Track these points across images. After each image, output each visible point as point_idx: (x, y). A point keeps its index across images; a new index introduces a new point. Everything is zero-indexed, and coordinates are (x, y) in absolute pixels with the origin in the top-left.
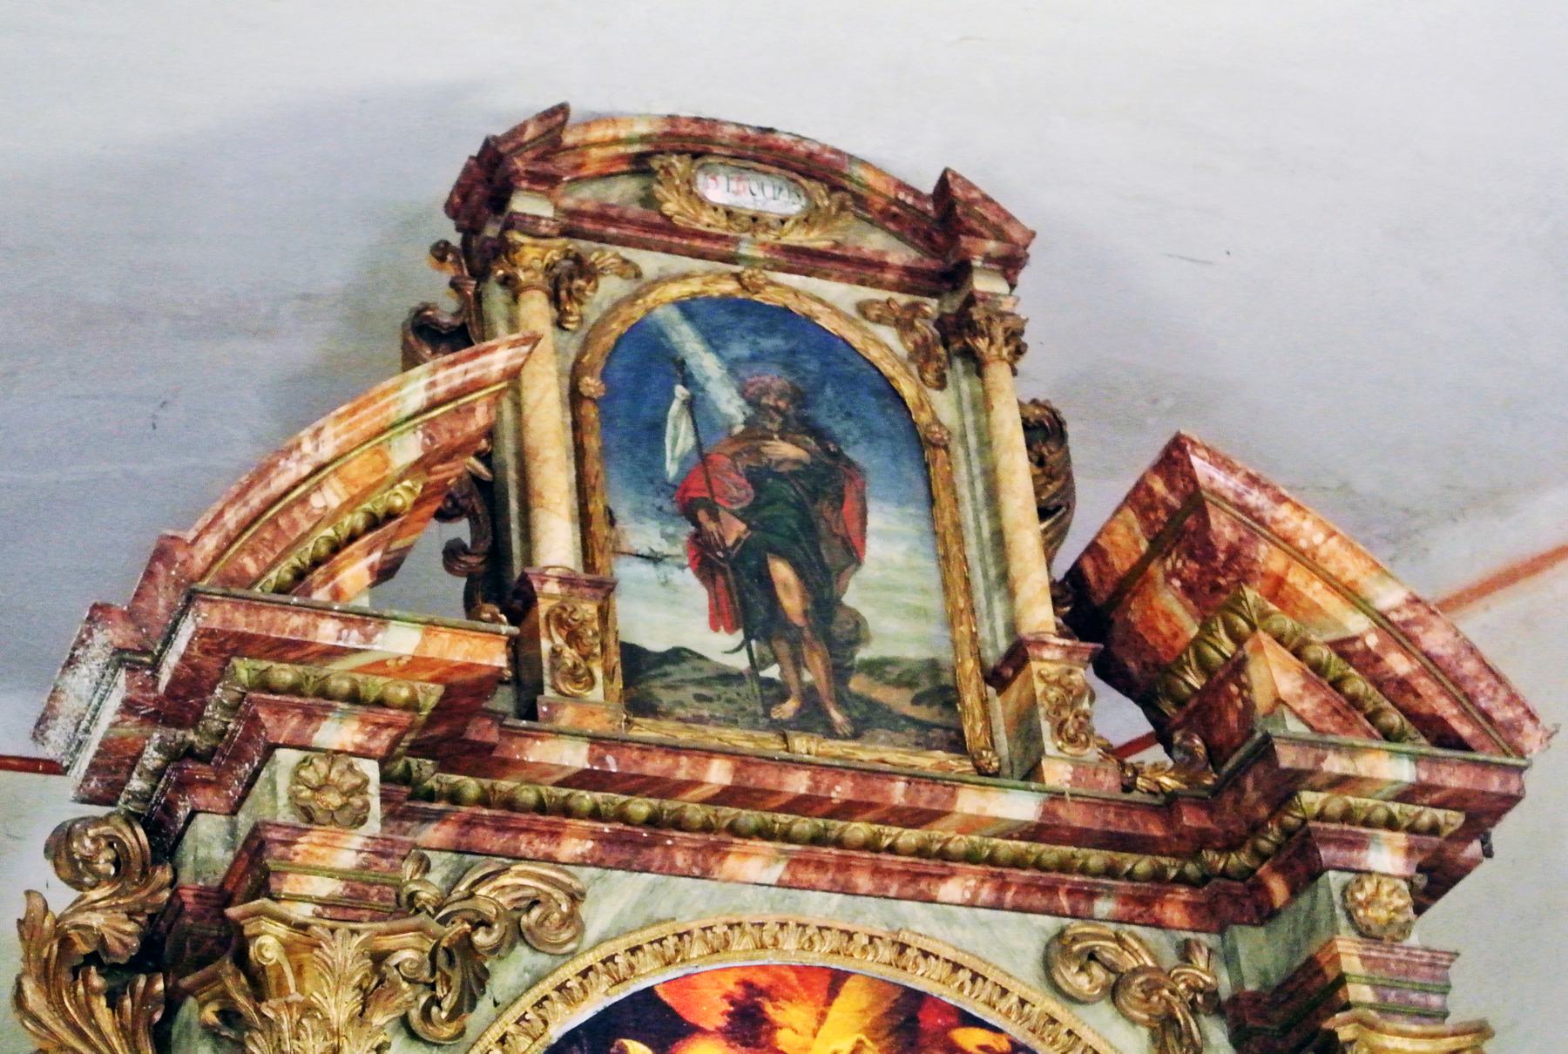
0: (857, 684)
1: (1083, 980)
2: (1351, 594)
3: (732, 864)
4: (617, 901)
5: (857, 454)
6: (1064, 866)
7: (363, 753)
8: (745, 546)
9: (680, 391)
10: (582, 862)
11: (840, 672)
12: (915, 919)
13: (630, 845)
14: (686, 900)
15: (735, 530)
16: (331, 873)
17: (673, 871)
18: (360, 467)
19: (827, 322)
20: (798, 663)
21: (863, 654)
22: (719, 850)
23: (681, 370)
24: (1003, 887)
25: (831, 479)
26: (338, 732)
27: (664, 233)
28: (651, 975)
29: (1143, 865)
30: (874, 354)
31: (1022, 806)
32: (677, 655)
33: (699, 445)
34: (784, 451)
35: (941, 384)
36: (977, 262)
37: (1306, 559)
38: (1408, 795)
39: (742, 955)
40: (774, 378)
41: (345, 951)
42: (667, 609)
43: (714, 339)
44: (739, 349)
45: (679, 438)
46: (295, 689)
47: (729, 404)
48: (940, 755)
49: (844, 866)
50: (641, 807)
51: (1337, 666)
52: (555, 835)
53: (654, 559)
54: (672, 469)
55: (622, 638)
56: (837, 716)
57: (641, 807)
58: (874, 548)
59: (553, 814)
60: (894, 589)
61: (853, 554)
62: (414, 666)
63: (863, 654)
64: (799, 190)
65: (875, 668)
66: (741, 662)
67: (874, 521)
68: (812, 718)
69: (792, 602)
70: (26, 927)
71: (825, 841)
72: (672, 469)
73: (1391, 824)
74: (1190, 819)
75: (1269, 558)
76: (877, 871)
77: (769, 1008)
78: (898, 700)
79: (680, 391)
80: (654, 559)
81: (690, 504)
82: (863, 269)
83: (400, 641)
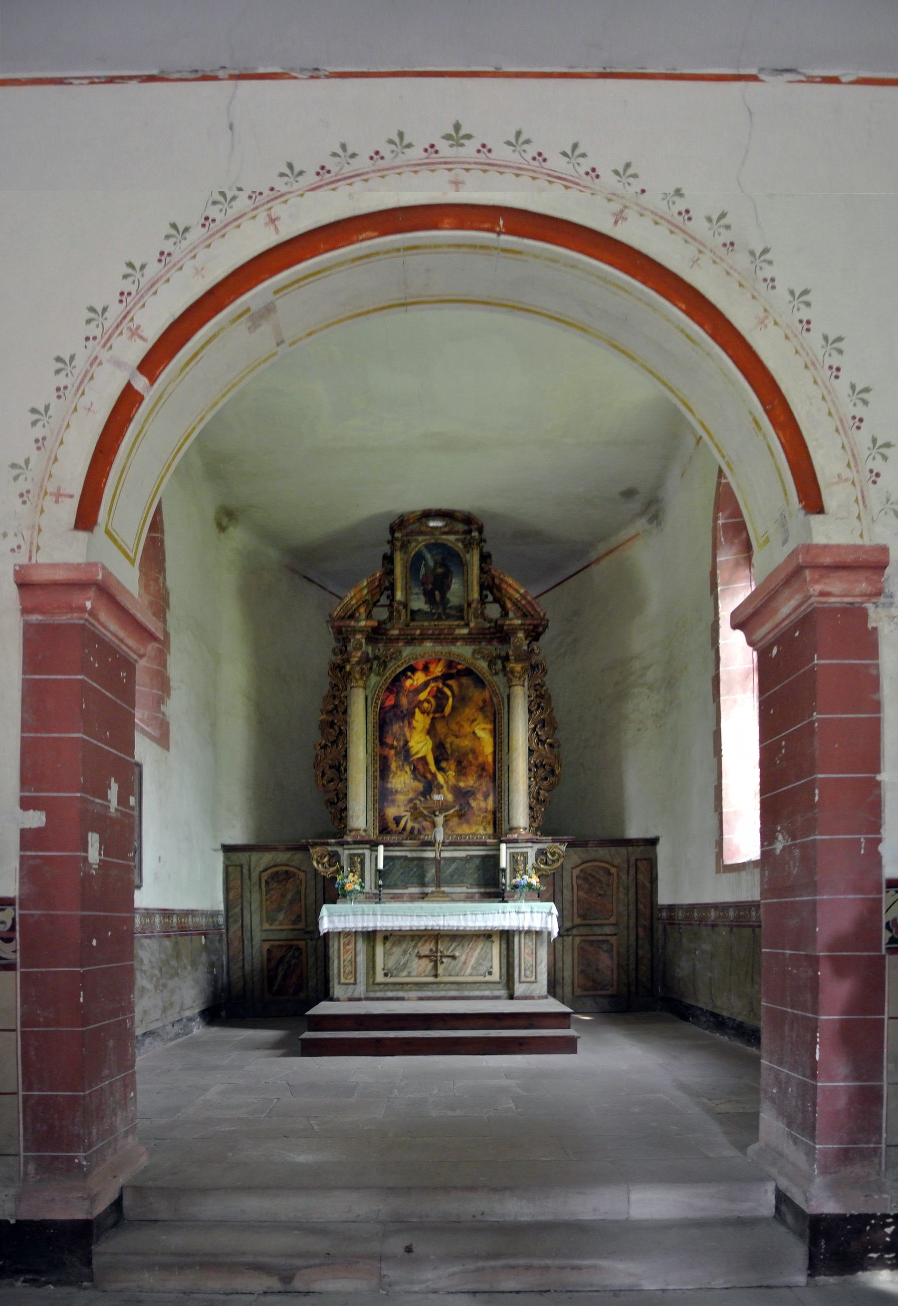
0: (447, 611)
4: (407, 651)
5: (452, 569)
11: (444, 609)
14: (418, 650)
15: (430, 586)
19: (450, 544)
23: (424, 558)
27: (421, 533)
28: (412, 662)
29: (489, 636)
31: (465, 631)
32: (419, 610)
34: (440, 570)
37: (510, 586)
38: (522, 624)
39: (427, 658)
40: (439, 557)
42: (419, 603)
43: (430, 552)
45: (423, 571)
47: (431, 563)
50: (409, 637)
53: (417, 594)
59: (397, 639)
61: (449, 588)
68: (440, 618)
69: (438, 598)
71: (438, 638)
73: (520, 629)
74: (492, 630)
75: (504, 586)
80: (417, 594)
81: (423, 584)
82: (456, 533)
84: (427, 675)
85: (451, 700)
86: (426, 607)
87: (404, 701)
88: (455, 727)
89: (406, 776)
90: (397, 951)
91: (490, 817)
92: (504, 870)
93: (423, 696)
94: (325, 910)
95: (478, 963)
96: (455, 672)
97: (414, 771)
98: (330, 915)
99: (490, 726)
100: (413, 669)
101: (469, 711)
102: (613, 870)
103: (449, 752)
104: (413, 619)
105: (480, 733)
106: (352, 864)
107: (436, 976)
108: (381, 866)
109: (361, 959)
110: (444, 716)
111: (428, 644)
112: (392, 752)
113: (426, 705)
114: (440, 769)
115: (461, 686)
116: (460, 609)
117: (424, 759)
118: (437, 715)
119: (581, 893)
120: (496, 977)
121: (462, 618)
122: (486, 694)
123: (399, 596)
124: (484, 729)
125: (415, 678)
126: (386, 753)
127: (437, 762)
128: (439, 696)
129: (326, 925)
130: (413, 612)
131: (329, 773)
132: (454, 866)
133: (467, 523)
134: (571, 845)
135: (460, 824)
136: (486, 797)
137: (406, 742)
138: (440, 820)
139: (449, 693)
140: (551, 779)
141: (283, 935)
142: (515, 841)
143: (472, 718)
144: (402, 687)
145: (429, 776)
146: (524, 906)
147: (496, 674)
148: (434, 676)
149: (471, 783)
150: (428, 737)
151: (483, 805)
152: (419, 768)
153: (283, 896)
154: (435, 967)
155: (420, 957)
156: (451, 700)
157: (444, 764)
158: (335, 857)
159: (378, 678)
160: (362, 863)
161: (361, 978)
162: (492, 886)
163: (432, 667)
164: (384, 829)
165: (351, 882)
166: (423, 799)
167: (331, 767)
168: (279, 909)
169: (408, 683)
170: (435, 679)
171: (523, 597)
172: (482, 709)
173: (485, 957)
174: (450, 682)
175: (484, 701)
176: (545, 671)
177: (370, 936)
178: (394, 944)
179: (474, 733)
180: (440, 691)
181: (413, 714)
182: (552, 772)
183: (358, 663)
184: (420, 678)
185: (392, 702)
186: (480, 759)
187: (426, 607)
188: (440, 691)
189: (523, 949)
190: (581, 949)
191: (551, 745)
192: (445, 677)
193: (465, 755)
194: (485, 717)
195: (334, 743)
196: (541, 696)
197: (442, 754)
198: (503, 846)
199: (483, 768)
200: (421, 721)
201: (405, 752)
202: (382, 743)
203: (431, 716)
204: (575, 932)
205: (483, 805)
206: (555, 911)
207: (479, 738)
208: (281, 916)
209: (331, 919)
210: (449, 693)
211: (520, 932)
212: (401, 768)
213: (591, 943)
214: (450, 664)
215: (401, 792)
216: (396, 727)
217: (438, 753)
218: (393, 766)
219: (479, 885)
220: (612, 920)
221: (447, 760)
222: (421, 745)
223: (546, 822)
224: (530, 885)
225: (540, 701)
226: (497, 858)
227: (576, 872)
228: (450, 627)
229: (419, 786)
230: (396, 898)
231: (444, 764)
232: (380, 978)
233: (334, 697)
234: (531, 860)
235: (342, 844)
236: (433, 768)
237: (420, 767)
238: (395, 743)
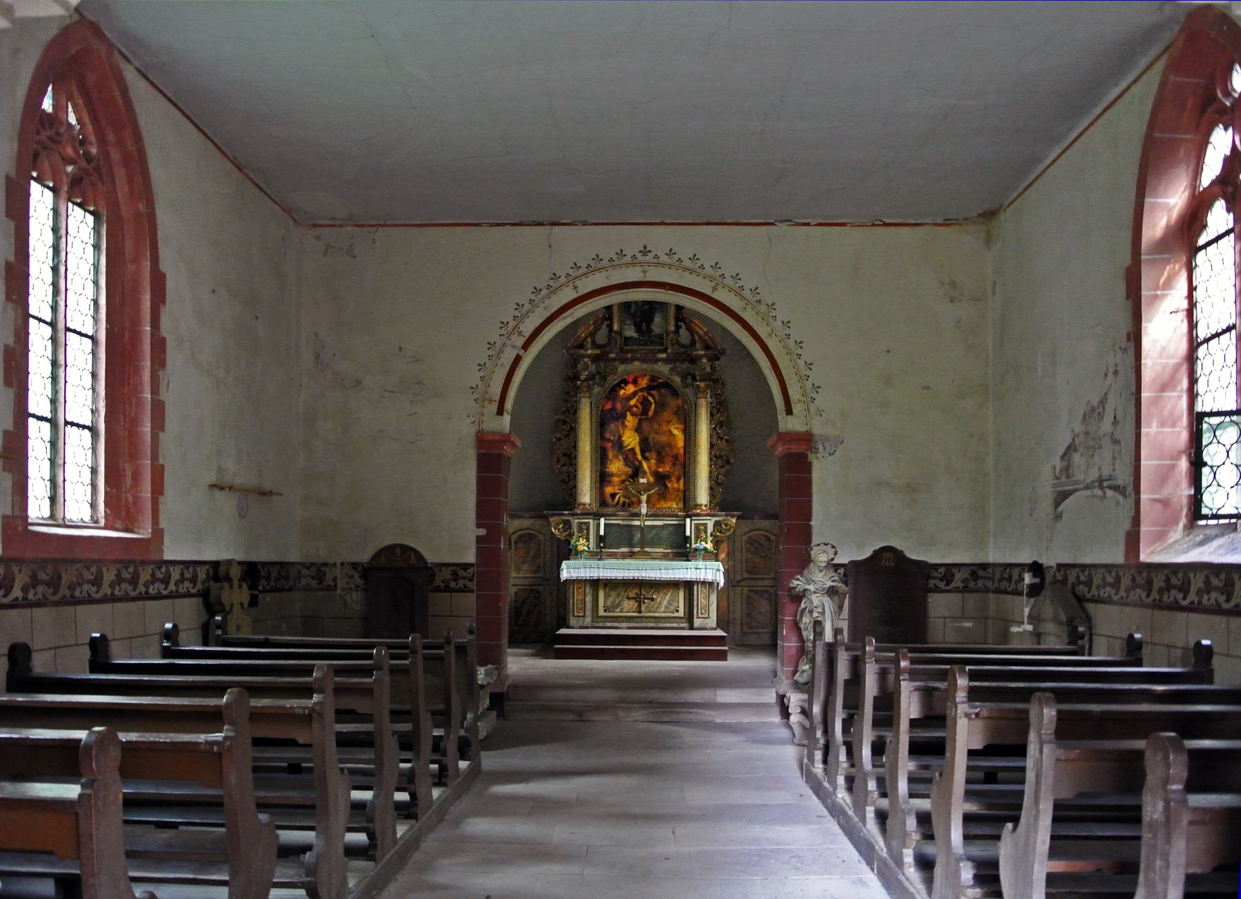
4: (621, 368)
14: (630, 367)
31: (664, 356)
42: (631, 332)
61: (653, 320)
68: (646, 344)
81: (633, 317)
86: (635, 335)
87: (619, 406)
90: (614, 594)
91: (681, 495)
92: (690, 538)
93: (633, 402)
94: (564, 564)
95: (669, 604)
96: (657, 384)
97: (625, 459)
98: (568, 568)
99: (681, 426)
100: (625, 382)
101: (667, 415)
102: (773, 538)
104: (626, 344)
105: (675, 432)
106: (580, 530)
107: (640, 612)
108: (602, 533)
109: (589, 599)
111: (637, 364)
114: (645, 458)
115: (661, 395)
116: (660, 337)
117: (633, 450)
119: (749, 555)
120: (681, 614)
121: (662, 344)
122: (680, 402)
123: (616, 327)
127: (643, 452)
128: (645, 403)
129: (564, 575)
130: (626, 339)
131: (563, 460)
132: (654, 532)
134: (739, 518)
135: (659, 500)
136: (678, 480)
137: (620, 437)
138: (644, 498)
140: (728, 467)
141: (526, 582)
142: (699, 515)
144: (618, 396)
146: (701, 564)
151: (676, 486)
152: (629, 457)
153: (528, 553)
154: (640, 606)
155: (629, 599)
157: (647, 454)
158: (568, 525)
160: (588, 529)
161: (588, 613)
162: (682, 550)
164: (603, 503)
165: (582, 545)
167: (564, 455)
168: (524, 563)
169: (622, 392)
170: (642, 390)
171: (706, 333)
172: (676, 413)
173: (674, 599)
175: (678, 408)
176: (724, 384)
177: (595, 583)
178: (611, 589)
180: (645, 399)
181: (625, 417)
182: (728, 462)
183: (586, 380)
184: (631, 389)
186: (675, 451)
187: (635, 335)
188: (645, 399)
189: (700, 594)
190: (749, 596)
191: (727, 441)
192: (649, 388)
193: (663, 447)
195: (566, 436)
196: (721, 403)
198: (688, 520)
199: (676, 457)
200: (631, 421)
201: (619, 445)
202: (602, 437)
204: (744, 583)
205: (676, 486)
206: (721, 568)
208: (525, 567)
209: (569, 570)
211: (697, 582)
212: (616, 457)
213: (756, 592)
214: (653, 378)
215: (616, 475)
216: (612, 426)
218: (610, 455)
219: (672, 547)
220: (772, 575)
222: (631, 439)
223: (723, 501)
224: (705, 549)
225: (719, 410)
226: (684, 525)
227: (745, 538)
228: (652, 351)
229: (629, 470)
230: (613, 556)
231: (647, 454)
232: (601, 613)
233: (566, 401)
234: (710, 529)
235: (573, 515)
236: (640, 457)
237: (630, 457)
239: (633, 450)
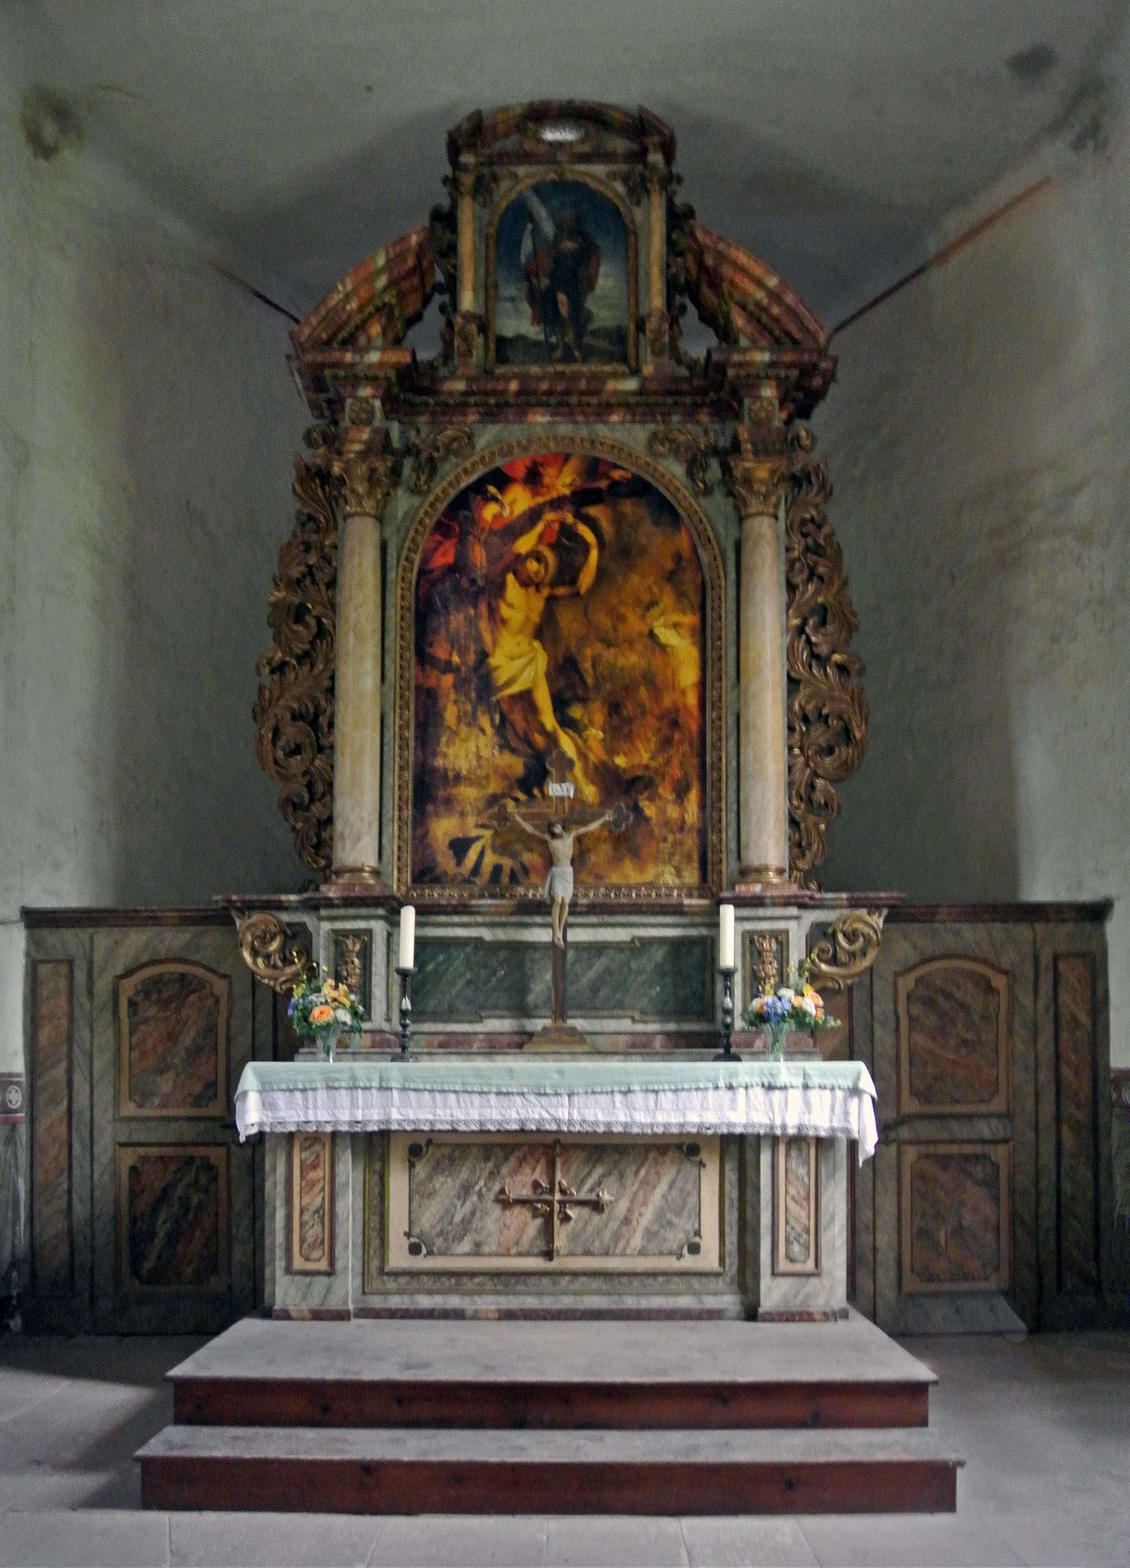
0: (588, 340)
1: (661, 448)
2: (760, 283)
3: (530, 418)
4: (487, 436)
5: (601, 242)
6: (657, 404)
7: (374, 397)
8: (548, 289)
9: (529, 226)
10: (475, 423)
11: (579, 336)
12: (602, 430)
13: (491, 415)
14: (514, 432)
15: (545, 282)
16: (360, 442)
17: (509, 422)
18: (364, 293)
19: (593, 185)
20: (563, 334)
21: (591, 327)
22: (524, 413)
23: (531, 218)
24: (634, 414)
25: (587, 256)
26: (365, 391)
27: (526, 157)
28: (499, 462)
29: (688, 400)
30: (610, 195)
31: (631, 385)
32: (519, 338)
33: (535, 248)
34: (569, 245)
35: (638, 203)
36: (651, 148)
37: (742, 270)
38: (772, 364)
39: (536, 451)
40: (568, 214)
41: (361, 469)
42: (518, 322)
43: (544, 201)
44: (555, 203)
45: (527, 246)
46: (346, 378)
47: (548, 228)
48: (615, 365)
49: (571, 413)
50: (492, 401)
51: (757, 312)
52: (465, 415)
53: (512, 299)
54: (523, 259)
55: (498, 333)
56: (577, 354)
57: (492, 401)
58: (601, 282)
59: (462, 406)
60: (605, 296)
61: (591, 286)
62: (381, 364)
63: (591, 327)
64: (579, 127)
65: (595, 333)
66: (542, 337)
67: (603, 269)
68: (568, 358)
69: (564, 310)
70: (297, 466)
72: (523, 259)
73: (768, 377)
74: (696, 382)
75: (727, 271)
76: (583, 413)
77: (541, 470)
78: (602, 344)
79: (529, 226)
80: (512, 299)
81: (528, 275)
82: (608, 157)
83: (374, 357)
84: (535, 493)
85: (594, 555)
86: (533, 331)
87: (479, 556)
88: (604, 621)
89: (483, 740)
90: (446, 1186)
91: (691, 842)
92: (728, 974)
93: (525, 544)
94: (251, 1076)
95: (662, 1220)
96: (600, 486)
97: (502, 727)
98: (265, 1089)
99: (690, 619)
100: (501, 479)
101: (637, 582)
102: (999, 982)
103: (590, 680)
104: (502, 360)
105: (667, 636)
106: (340, 957)
107: (549, 1254)
108: (407, 959)
109: (349, 1205)
110: (578, 594)
111: (540, 418)
112: (448, 680)
113: (533, 566)
114: (566, 722)
115: (618, 520)
116: (618, 336)
117: (526, 698)
118: (561, 591)
119: (921, 1040)
120: (709, 1259)
121: (624, 359)
122: (682, 541)
123: (468, 301)
124: (676, 626)
125: (507, 499)
126: (432, 682)
127: (560, 705)
128: (566, 545)
129: (251, 1116)
130: (502, 342)
131: (292, 732)
132: (599, 965)
133: (640, 138)
134: (897, 915)
135: (616, 861)
136: (681, 792)
137: (484, 656)
138: (564, 847)
139: (589, 536)
140: (844, 752)
141: (171, 1133)
142: (757, 902)
143: (646, 598)
144: (474, 521)
145: (539, 740)
146: (786, 1070)
147: (708, 491)
148: (554, 495)
149: (645, 757)
150: (537, 644)
151: (673, 812)
152: (512, 719)
153: (172, 1038)
154: (548, 1232)
155: (505, 1203)
156: (594, 555)
158: (297, 939)
159: (416, 500)
160: (366, 955)
161: (349, 1258)
162: (696, 1016)
163: (549, 475)
164: (425, 873)
165: (329, 1003)
166: (522, 796)
167: (296, 717)
168: (162, 1070)
169: (490, 511)
170: (557, 504)
171: (775, 296)
172: (671, 577)
173: (683, 1204)
174: (593, 511)
175: (678, 558)
176: (826, 490)
177: (373, 1145)
178: (437, 1168)
179: (652, 635)
180: (567, 531)
181: (502, 587)
182: (847, 732)
183: (363, 455)
184: (518, 500)
185: (450, 559)
186: (667, 701)
187: (533, 331)
188: (567, 531)
189: (781, 1183)
190: (920, 1176)
191: (842, 668)
192: (581, 498)
193: (630, 688)
194: (680, 595)
195: (305, 657)
196: (816, 550)
197: (571, 686)
198: (728, 912)
199: (672, 719)
200: (519, 603)
201: (481, 681)
202: (423, 657)
203: (546, 592)
204: (904, 1133)
205: (673, 812)
206: (867, 1084)
207: (663, 648)
208: (166, 1084)
209: (265, 1099)
210: (589, 536)
211: (774, 1140)
212: (471, 721)
213: (945, 1161)
214: (594, 467)
215: (470, 781)
216: (457, 620)
217: (561, 683)
218: (450, 714)
219: (664, 1014)
220: (998, 1104)
221: (583, 701)
222: (520, 664)
223: (826, 860)
224: (798, 1015)
225: (814, 560)
227: (907, 983)
228: (593, 377)
229: (517, 765)
230: (453, 1045)
231: (576, 712)
232: (398, 1257)
233: (308, 547)
234: (796, 952)
235: (313, 906)
236: (549, 720)
237: (517, 717)
238: (456, 659)
239: (526, 698)
